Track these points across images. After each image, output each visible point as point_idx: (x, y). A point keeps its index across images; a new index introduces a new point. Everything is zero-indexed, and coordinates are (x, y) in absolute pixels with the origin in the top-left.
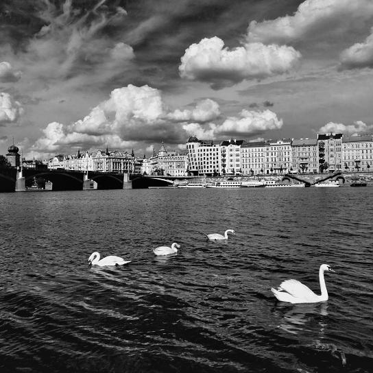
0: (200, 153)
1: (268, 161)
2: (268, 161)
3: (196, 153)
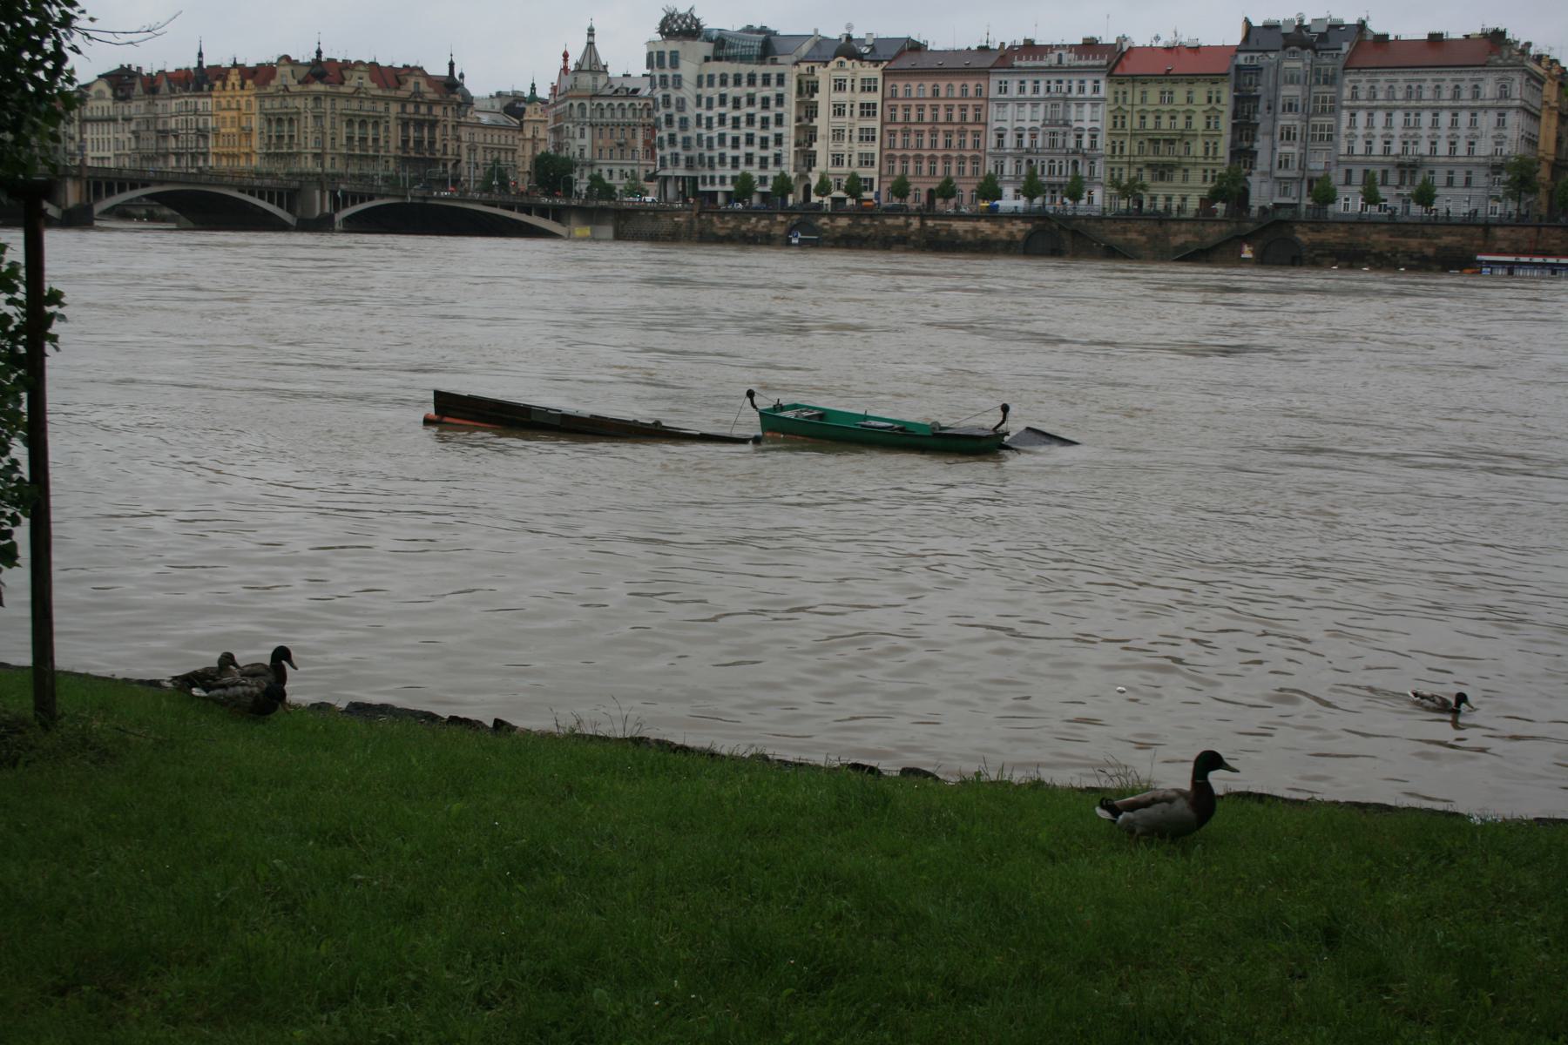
0: (707, 92)
1: (1000, 144)
2: (1000, 144)
3: (688, 91)
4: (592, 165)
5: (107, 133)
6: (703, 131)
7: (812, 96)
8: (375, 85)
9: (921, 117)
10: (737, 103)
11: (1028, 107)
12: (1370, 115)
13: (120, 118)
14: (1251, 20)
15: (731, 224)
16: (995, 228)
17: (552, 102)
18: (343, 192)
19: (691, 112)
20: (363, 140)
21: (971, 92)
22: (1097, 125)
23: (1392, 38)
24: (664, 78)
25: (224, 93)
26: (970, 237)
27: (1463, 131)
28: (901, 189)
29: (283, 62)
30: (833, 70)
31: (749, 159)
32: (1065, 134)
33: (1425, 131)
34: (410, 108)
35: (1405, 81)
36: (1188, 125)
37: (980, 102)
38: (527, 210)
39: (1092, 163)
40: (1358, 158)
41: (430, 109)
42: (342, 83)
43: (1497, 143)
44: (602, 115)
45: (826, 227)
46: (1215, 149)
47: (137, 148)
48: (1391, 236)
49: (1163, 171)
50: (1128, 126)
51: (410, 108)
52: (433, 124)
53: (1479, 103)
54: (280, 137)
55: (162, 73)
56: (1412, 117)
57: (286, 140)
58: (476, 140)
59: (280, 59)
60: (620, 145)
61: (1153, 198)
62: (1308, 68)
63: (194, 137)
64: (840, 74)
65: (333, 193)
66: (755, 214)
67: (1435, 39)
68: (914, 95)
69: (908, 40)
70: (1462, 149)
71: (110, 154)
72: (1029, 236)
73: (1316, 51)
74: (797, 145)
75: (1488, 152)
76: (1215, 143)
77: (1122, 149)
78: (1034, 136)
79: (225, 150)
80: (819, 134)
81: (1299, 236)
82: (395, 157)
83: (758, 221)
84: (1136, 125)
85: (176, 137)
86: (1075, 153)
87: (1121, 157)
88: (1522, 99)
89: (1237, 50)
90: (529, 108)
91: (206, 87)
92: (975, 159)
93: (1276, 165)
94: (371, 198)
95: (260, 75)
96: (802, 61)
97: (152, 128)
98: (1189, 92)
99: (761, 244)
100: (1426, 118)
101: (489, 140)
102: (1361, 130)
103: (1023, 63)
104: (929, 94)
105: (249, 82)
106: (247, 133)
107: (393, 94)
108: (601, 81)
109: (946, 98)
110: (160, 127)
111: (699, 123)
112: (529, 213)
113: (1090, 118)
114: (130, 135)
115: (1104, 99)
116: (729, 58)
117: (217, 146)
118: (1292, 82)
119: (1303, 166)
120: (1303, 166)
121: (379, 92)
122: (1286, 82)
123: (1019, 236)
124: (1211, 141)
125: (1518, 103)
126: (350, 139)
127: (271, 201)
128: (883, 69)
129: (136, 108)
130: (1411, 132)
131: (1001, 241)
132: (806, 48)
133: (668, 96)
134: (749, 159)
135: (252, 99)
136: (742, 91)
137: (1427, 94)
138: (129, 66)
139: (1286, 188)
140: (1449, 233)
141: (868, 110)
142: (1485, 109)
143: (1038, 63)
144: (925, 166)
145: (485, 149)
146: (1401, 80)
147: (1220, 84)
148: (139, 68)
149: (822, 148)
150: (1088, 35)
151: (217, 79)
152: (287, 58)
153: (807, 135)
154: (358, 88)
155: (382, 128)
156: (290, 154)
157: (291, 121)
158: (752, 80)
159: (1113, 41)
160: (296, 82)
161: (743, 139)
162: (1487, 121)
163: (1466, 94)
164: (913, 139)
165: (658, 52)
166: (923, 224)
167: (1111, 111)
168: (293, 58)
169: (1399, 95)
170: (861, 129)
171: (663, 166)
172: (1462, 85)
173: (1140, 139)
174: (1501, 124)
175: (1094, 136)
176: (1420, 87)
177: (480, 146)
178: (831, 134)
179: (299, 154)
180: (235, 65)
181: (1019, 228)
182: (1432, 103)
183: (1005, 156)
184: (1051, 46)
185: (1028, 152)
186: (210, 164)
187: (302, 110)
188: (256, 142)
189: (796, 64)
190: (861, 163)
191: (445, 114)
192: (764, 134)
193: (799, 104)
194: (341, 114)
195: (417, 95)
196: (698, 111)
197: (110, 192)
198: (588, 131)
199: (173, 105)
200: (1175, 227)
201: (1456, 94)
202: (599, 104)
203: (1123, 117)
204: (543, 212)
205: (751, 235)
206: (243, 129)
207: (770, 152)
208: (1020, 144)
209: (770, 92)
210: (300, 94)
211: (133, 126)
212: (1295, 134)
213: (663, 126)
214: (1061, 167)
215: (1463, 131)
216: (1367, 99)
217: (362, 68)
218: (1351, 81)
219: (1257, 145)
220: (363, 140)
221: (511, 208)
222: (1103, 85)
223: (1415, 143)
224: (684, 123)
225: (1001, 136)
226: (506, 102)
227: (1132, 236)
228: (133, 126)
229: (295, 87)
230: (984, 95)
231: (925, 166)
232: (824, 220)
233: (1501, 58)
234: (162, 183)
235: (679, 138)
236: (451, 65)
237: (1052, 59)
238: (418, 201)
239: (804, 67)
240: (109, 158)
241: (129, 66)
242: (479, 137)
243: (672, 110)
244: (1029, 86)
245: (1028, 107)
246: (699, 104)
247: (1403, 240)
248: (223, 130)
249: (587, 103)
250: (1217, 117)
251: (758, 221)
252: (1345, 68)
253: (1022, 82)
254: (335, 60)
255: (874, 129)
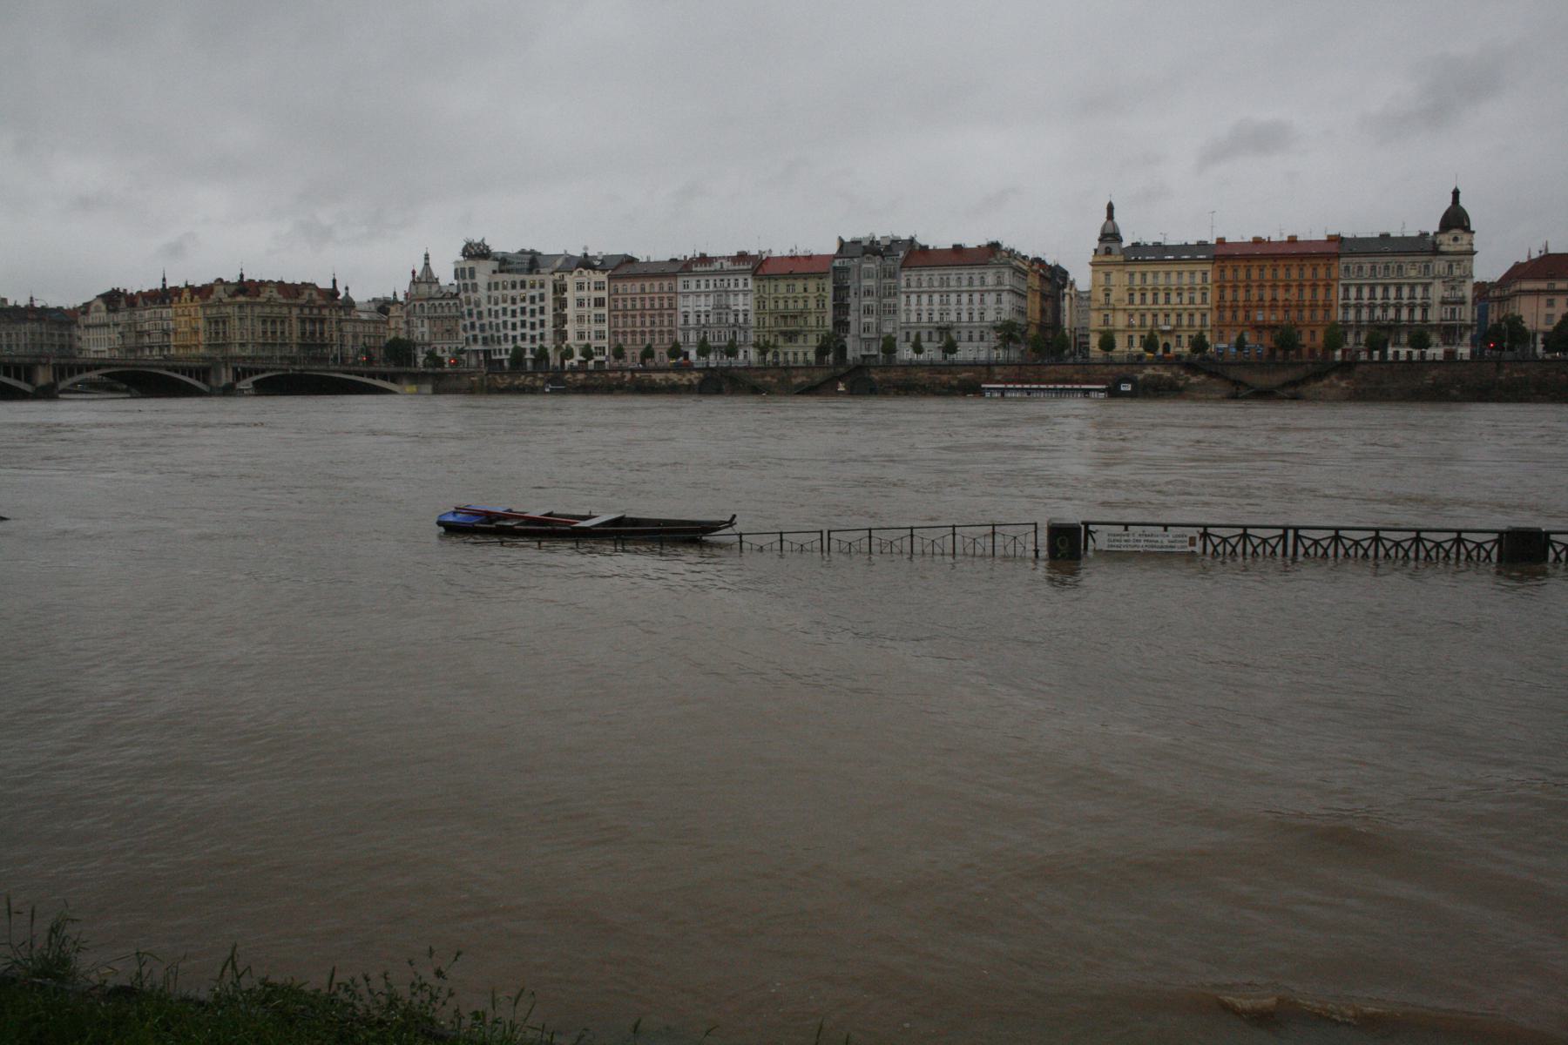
1: (686, 322)
2: (686, 322)
3: (482, 293)
4: (429, 345)
5: (103, 334)
6: (493, 319)
7: (563, 294)
8: (281, 296)
9: (634, 306)
10: (514, 301)
11: (703, 298)
12: (919, 296)
13: (111, 323)
14: (843, 238)
15: (508, 381)
16: (680, 377)
17: (405, 303)
18: (242, 368)
19: (484, 307)
20: (274, 333)
21: (666, 289)
22: (747, 308)
23: (931, 248)
24: (465, 285)
25: (179, 305)
26: (664, 383)
27: (976, 306)
28: (619, 353)
29: (219, 283)
30: (576, 277)
31: (523, 337)
32: (727, 314)
33: (953, 307)
34: (306, 311)
35: (939, 275)
36: (806, 306)
37: (671, 295)
38: (372, 375)
39: (746, 332)
40: (913, 325)
41: (320, 311)
42: (258, 296)
43: (998, 313)
44: (435, 312)
45: (570, 380)
46: (823, 322)
47: (123, 344)
48: (931, 374)
49: (790, 336)
50: (767, 308)
51: (306, 311)
52: (322, 321)
53: (985, 288)
54: (217, 333)
55: (139, 293)
56: (945, 298)
57: (221, 335)
58: (358, 330)
59: (216, 281)
60: (448, 331)
61: (786, 354)
62: (879, 268)
63: (161, 335)
64: (580, 279)
65: (235, 369)
66: (523, 374)
67: (958, 249)
68: (629, 291)
69: (626, 256)
70: (976, 317)
71: (106, 349)
72: (703, 382)
73: (883, 257)
74: (555, 326)
75: (993, 319)
76: (823, 317)
77: (764, 323)
78: (707, 316)
79: (181, 343)
80: (569, 318)
81: (874, 376)
82: (298, 344)
83: (525, 379)
84: (772, 306)
85: (149, 335)
86: (734, 326)
87: (764, 327)
88: (1010, 285)
89: (835, 257)
90: (393, 309)
91: (168, 301)
92: (670, 332)
93: (862, 330)
94: (263, 371)
95: (203, 292)
96: (557, 271)
97: (133, 329)
98: (805, 285)
99: (528, 393)
100: (953, 298)
101: (367, 329)
102: (913, 307)
103: (699, 269)
104: (638, 290)
105: (196, 297)
106: (196, 331)
107: (290, 301)
108: (434, 288)
109: (650, 293)
110: (138, 329)
111: (490, 315)
112: (374, 378)
113: (743, 303)
114: (118, 335)
115: (752, 291)
116: (509, 271)
117: (176, 341)
118: (868, 277)
119: (879, 330)
120: (879, 330)
121: (284, 301)
122: (865, 278)
123: (696, 382)
124: (820, 316)
125: (1008, 287)
126: (265, 333)
127: (191, 376)
128: (609, 275)
129: (121, 317)
130: (944, 307)
131: (683, 385)
132: (559, 263)
133: (469, 297)
134: (523, 337)
135: (199, 308)
136: (518, 292)
137: (953, 283)
138: (118, 289)
139: (869, 345)
140: (966, 371)
141: (599, 302)
142: (989, 291)
143: (708, 268)
144: (638, 337)
145: (364, 336)
146: (937, 274)
147: (824, 280)
148: (125, 290)
149: (571, 328)
150: (741, 249)
151: (175, 296)
152: (220, 280)
153: (561, 319)
154: (269, 299)
155: (287, 325)
156: (224, 345)
157: (224, 323)
158: (523, 285)
159: (757, 253)
160: (226, 296)
161: (519, 324)
162: (990, 299)
163: (977, 282)
164: (629, 320)
165: (461, 269)
166: (633, 377)
167: (756, 298)
168: (225, 280)
169: (936, 284)
170: (596, 315)
171: (467, 344)
172: (974, 277)
173: (776, 315)
174: (999, 301)
175: (746, 315)
176: (948, 279)
177: (361, 335)
178: (576, 319)
179: (231, 343)
180: (187, 286)
181: (694, 377)
182: (956, 289)
183: (689, 329)
184: (716, 258)
185: (704, 326)
186: (172, 353)
187: (231, 314)
188: (202, 337)
189: (552, 273)
190: (596, 337)
191: (330, 314)
192: (533, 320)
193: (555, 299)
194: (258, 317)
195: (310, 304)
196: (489, 306)
197: (71, 374)
198: (426, 322)
199: (147, 314)
200: (794, 372)
201: (971, 283)
202: (433, 304)
203: (764, 302)
204: (384, 377)
205: (521, 387)
206: (193, 328)
207: (537, 332)
208: (698, 321)
209: (535, 292)
210: (229, 304)
211: (120, 329)
212: (872, 311)
213: (467, 317)
214: (725, 336)
215: (976, 306)
216: (939, 286)
217: (272, 285)
218: (906, 276)
219: (849, 318)
220: (274, 333)
221: (362, 375)
222: (750, 281)
223: (948, 314)
224: (480, 314)
225: (686, 316)
226: (381, 303)
227: (768, 379)
228: (120, 329)
229: (226, 300)
230: (674, 290)
231: (638, 337)
232: (569, 376)
233: (996, 259)
234: (109, 366)
235: (477, 325)
236: (334, 281)
237: (717, 266)
238: (297, 373)
239: (557, 275)
240: (104, 351)
241: (118, 289)
242: (360, 328)
243: (472, 306)
244: (703, 283)
245: (703, 298)
246: (489, 302)
247: (938, 376)
248: (179, 330)
249: (425, 303)
250: (823, 301)
251: (525, 379)
252: (901, 267)
253: (698, 281)
254: (253, 281)
255: (604, 315)
